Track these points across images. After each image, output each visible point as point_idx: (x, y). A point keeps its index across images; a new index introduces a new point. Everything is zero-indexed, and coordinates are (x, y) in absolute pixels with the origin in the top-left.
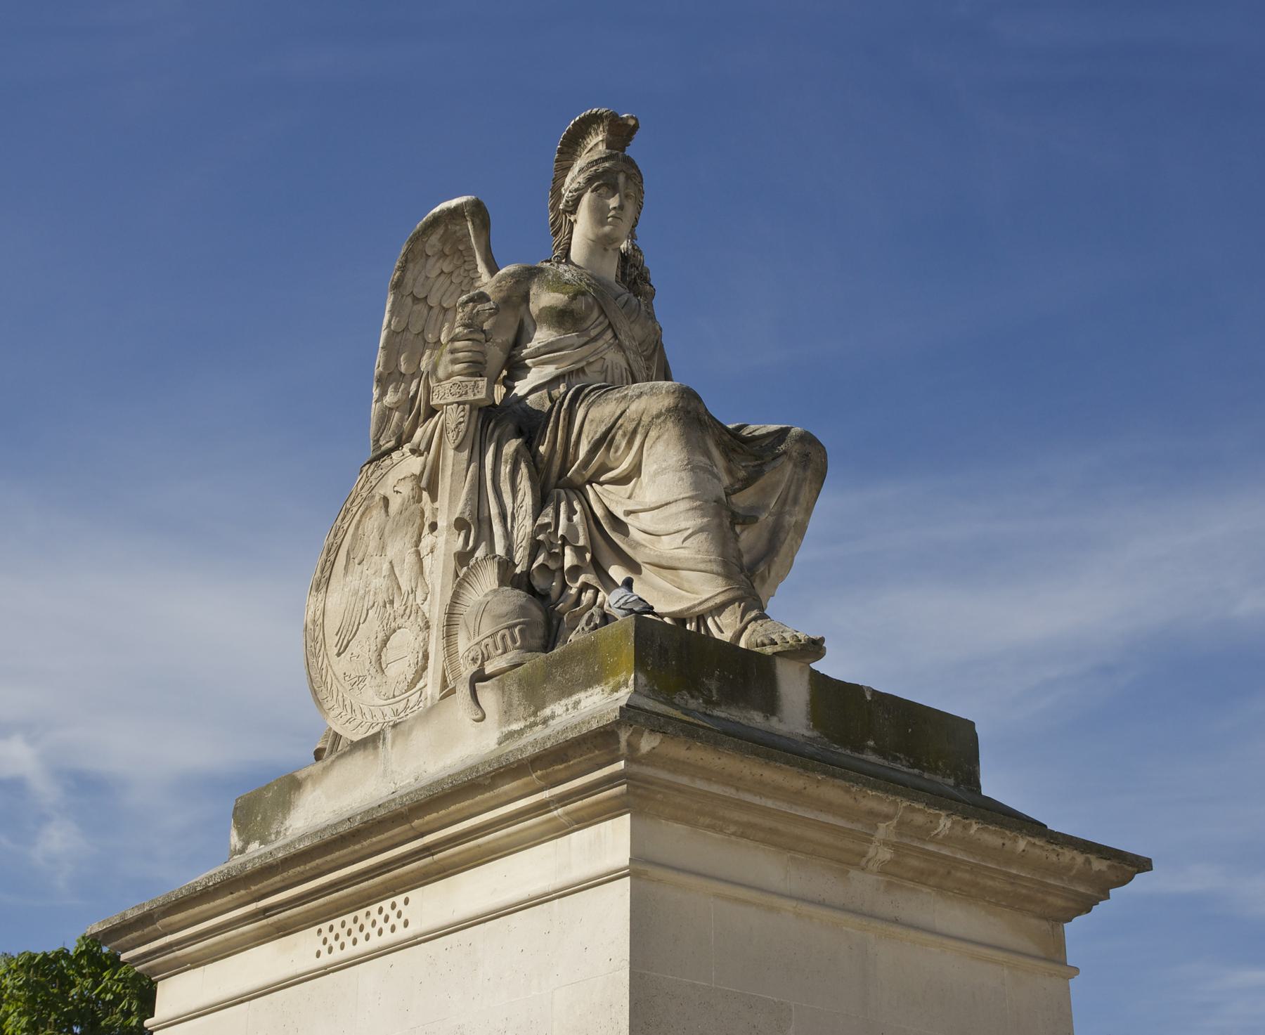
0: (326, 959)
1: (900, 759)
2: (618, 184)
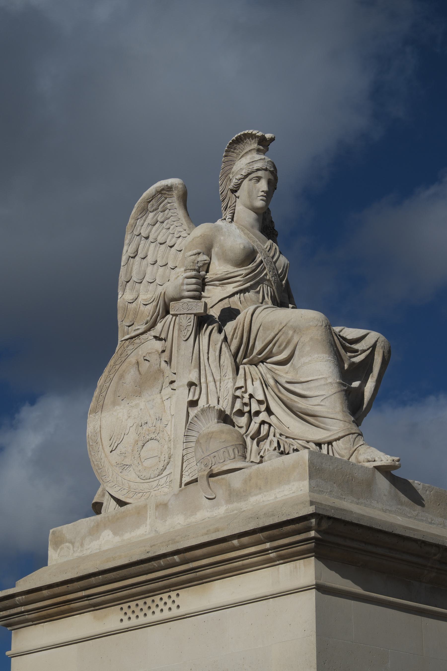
0: (126, 624)
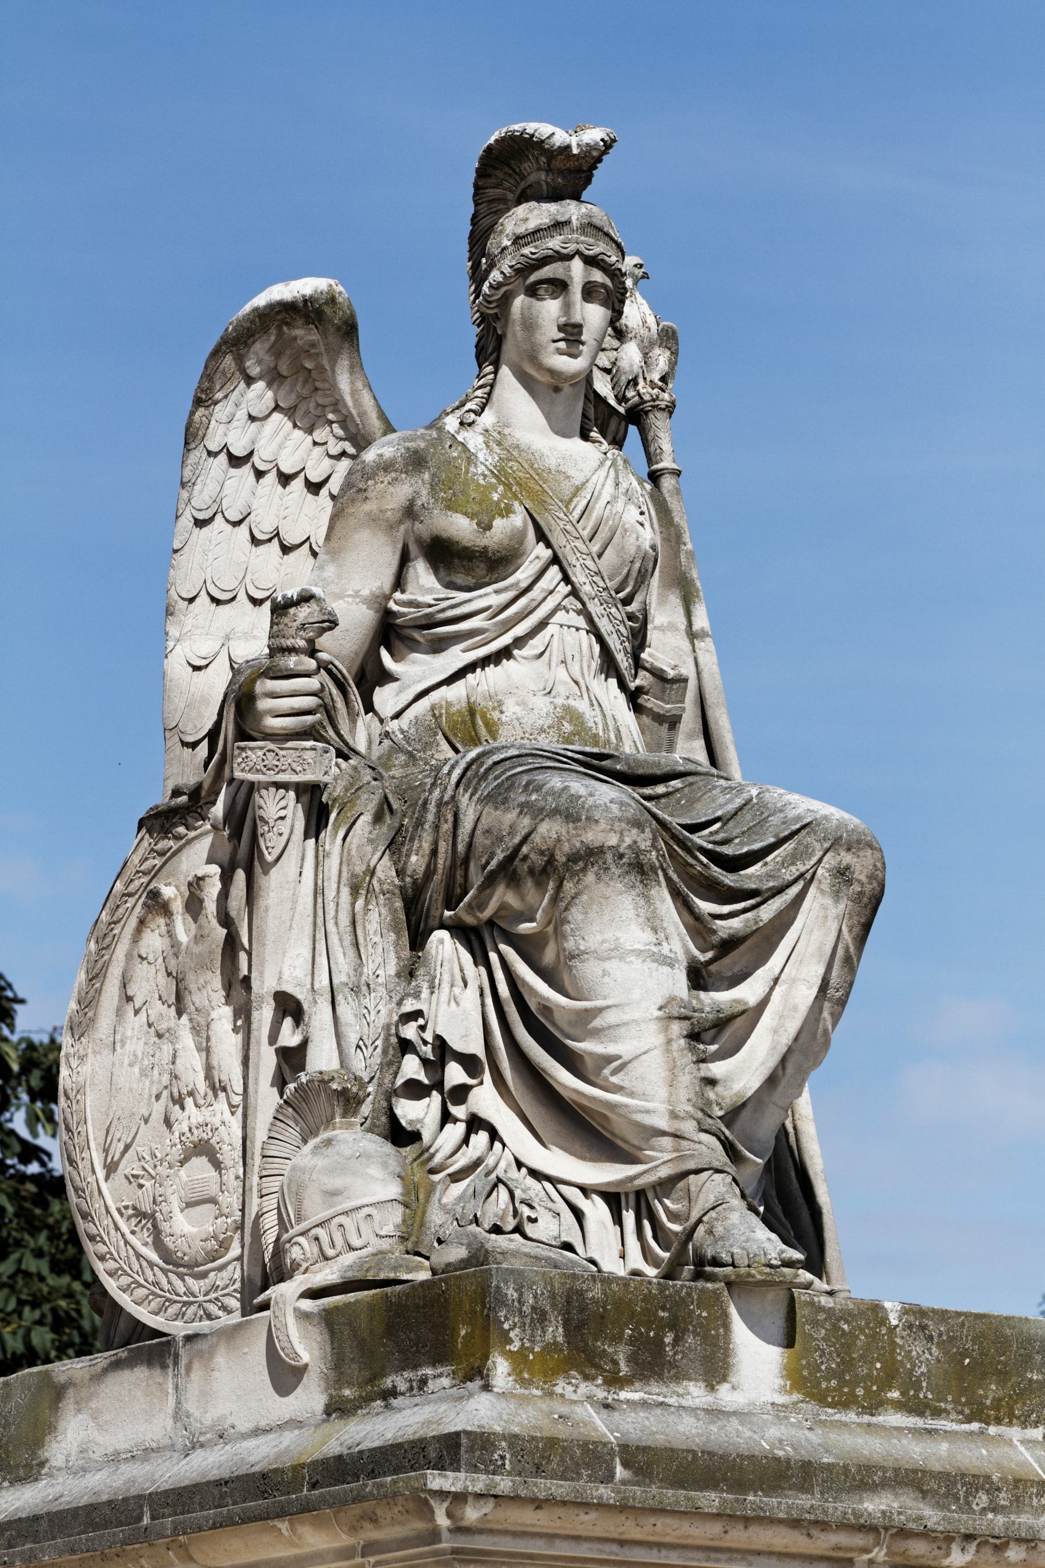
1: (945, 1411)
2: (571, 277)
